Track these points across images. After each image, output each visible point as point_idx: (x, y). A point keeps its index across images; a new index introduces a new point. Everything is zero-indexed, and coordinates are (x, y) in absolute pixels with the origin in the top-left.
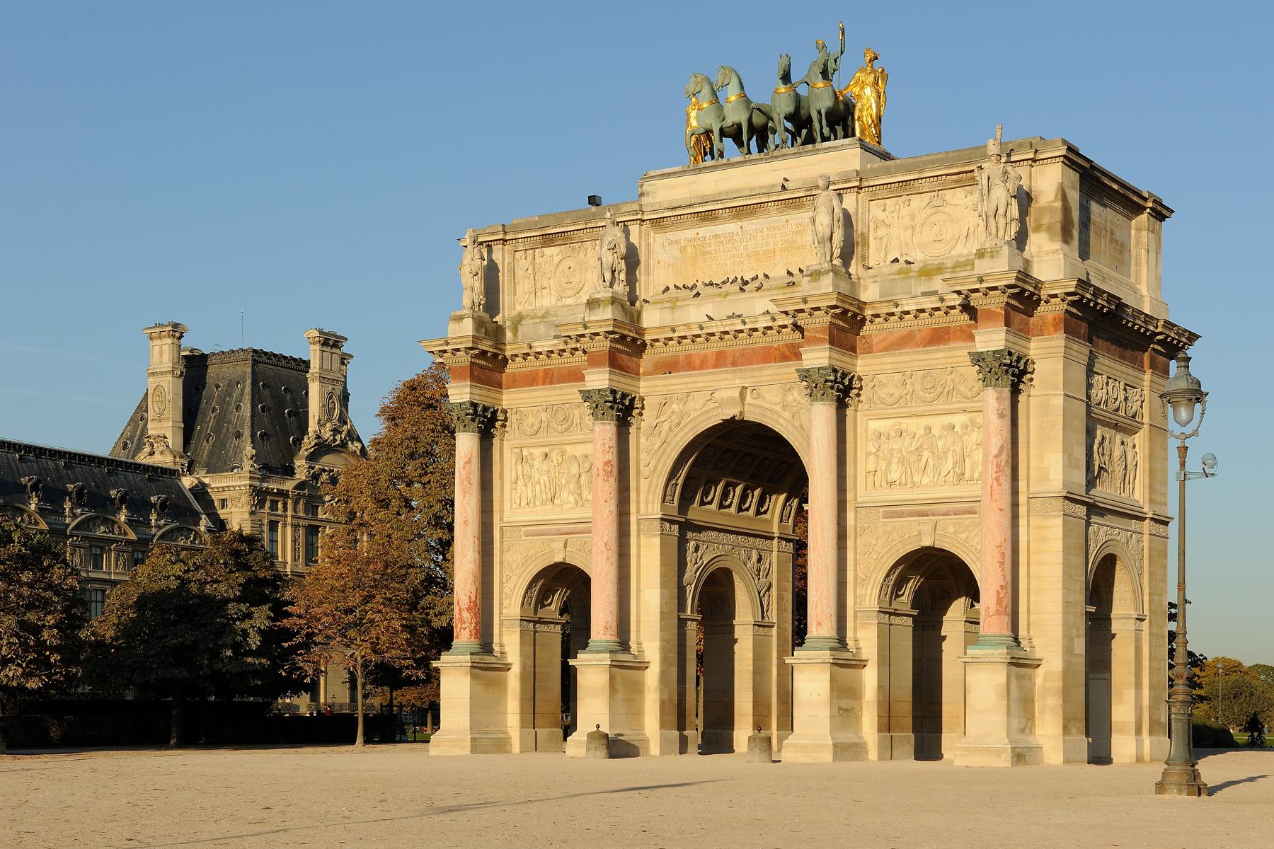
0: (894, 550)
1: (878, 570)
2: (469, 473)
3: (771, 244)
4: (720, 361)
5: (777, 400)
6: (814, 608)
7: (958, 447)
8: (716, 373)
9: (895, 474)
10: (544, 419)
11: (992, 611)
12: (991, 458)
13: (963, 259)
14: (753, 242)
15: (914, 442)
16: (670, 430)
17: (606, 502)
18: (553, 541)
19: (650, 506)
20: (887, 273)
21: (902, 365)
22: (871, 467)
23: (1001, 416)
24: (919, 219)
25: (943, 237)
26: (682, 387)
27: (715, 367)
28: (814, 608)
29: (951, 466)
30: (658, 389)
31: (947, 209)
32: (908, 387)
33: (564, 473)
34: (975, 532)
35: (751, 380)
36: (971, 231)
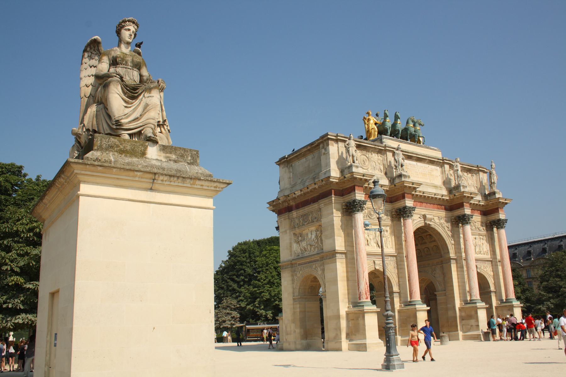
10: (366, 212)
27: (420, 207)
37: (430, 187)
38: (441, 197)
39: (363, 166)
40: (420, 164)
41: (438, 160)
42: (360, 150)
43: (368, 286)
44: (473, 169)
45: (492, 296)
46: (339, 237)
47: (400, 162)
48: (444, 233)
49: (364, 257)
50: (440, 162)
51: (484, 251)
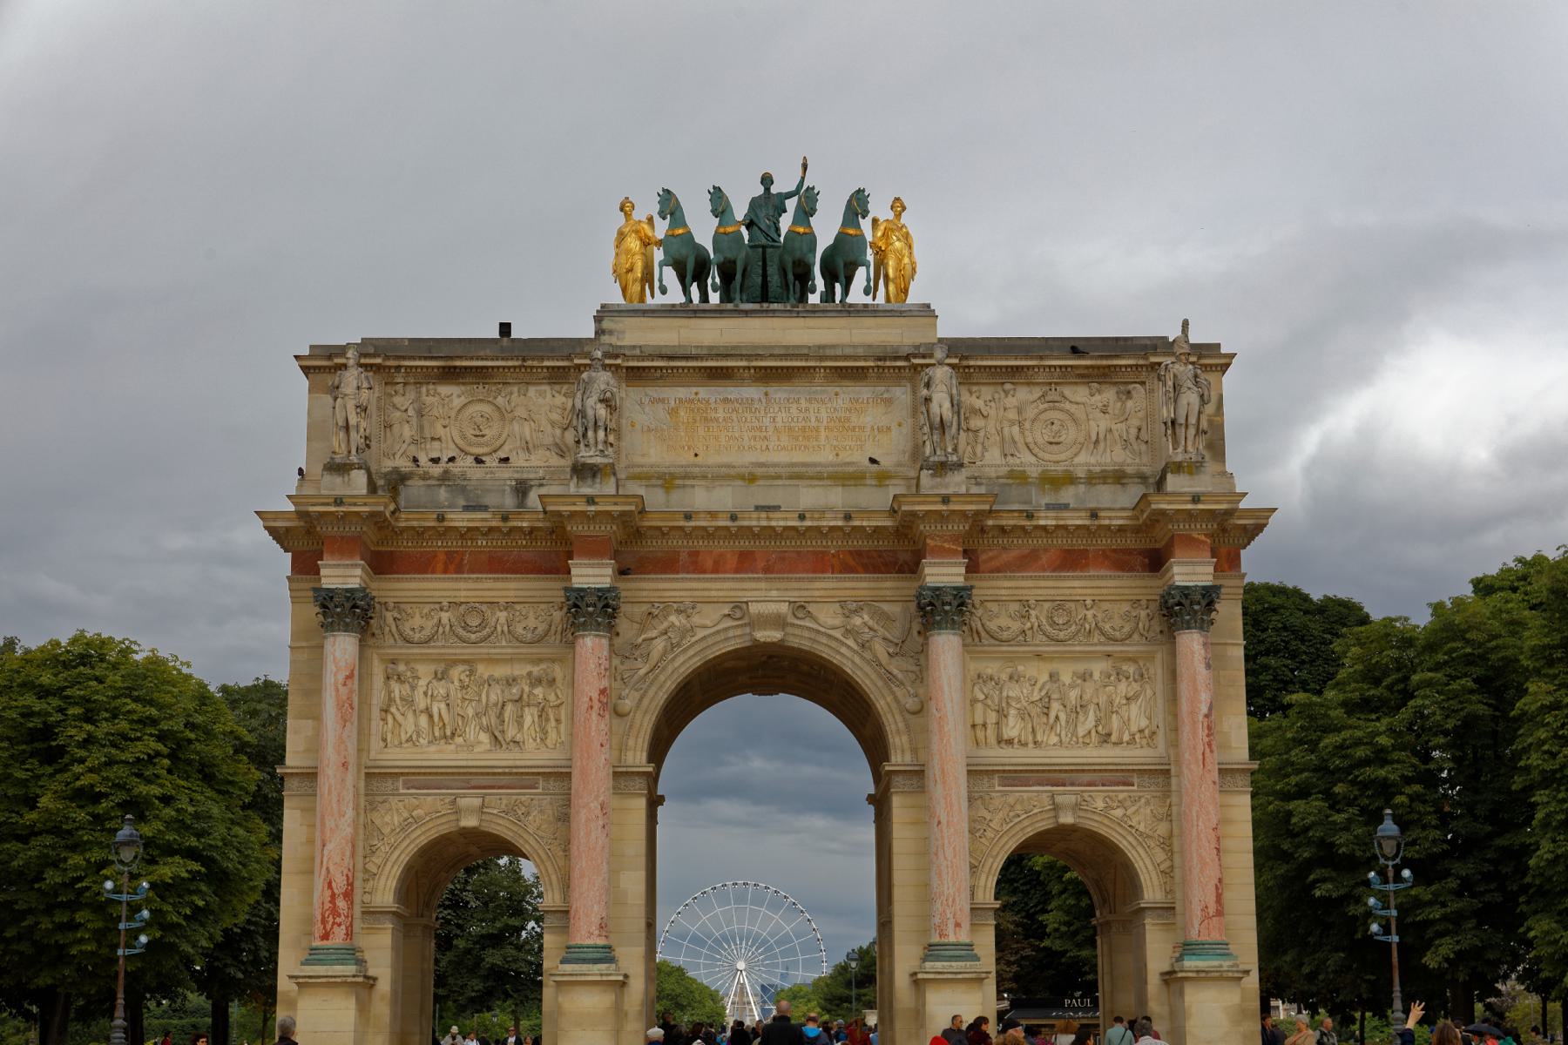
0: (1017, 828)
1: (994, 854)
2: (351, 692)
3: (813, 419)
4: (745, 563)
5: (837, 622)
6: (950, 904)
7: (1102, 700)
8: (742, 580)
9: (1013, 728)
10: (445, 621)
11: (1212, 910)
12: (1201, 718)
13: (1098, 469)
14: (784, 415)
15: (1035, 694)
16: (665, 653)
17: (602, 745)
18: (465, 796)
19: (630, 755)
20: (994, 475)
21: (1024, 592)
22: (979, 720)
23: (1208, 666)
24: (1030, 413)
25: (1061, 439)
26: (682, 593)
27: (737, 571)
28: (950, 904)
29: (1093, 723)
30: (645, 593)
31: (1067, 406)
32: (1033, 619)
33: (471, 700)
34: (1134, 809)
35: (796, 593)
36: (1101, 436)
37: (816, 482)
38: (840, 523)
39: (470, 445)
40: (779, 392)
41: (880, 363)
42: (463, 384)
43: (333, 896)
44: (1115, 366)
45: (1147, 927)
46: (304, 721)
47: (590, 413)
48: (867, 669)
49: (330, 792)
50: (900, 368)
51: (1134, 729)
